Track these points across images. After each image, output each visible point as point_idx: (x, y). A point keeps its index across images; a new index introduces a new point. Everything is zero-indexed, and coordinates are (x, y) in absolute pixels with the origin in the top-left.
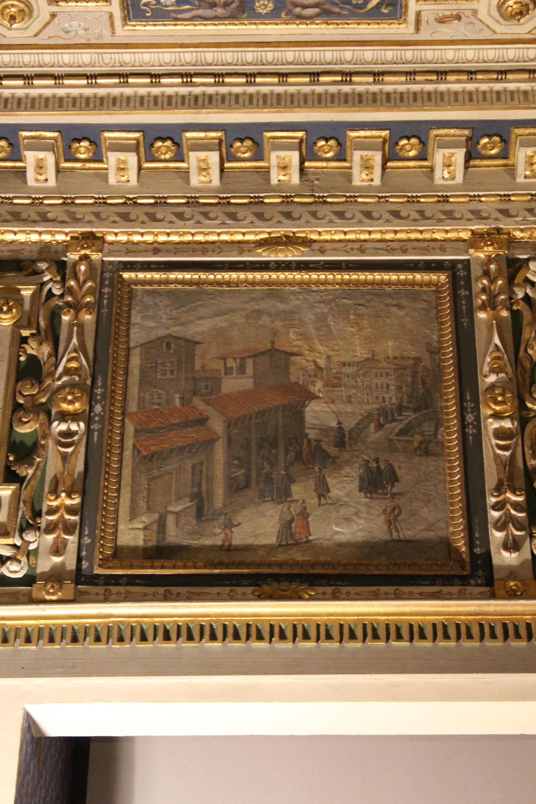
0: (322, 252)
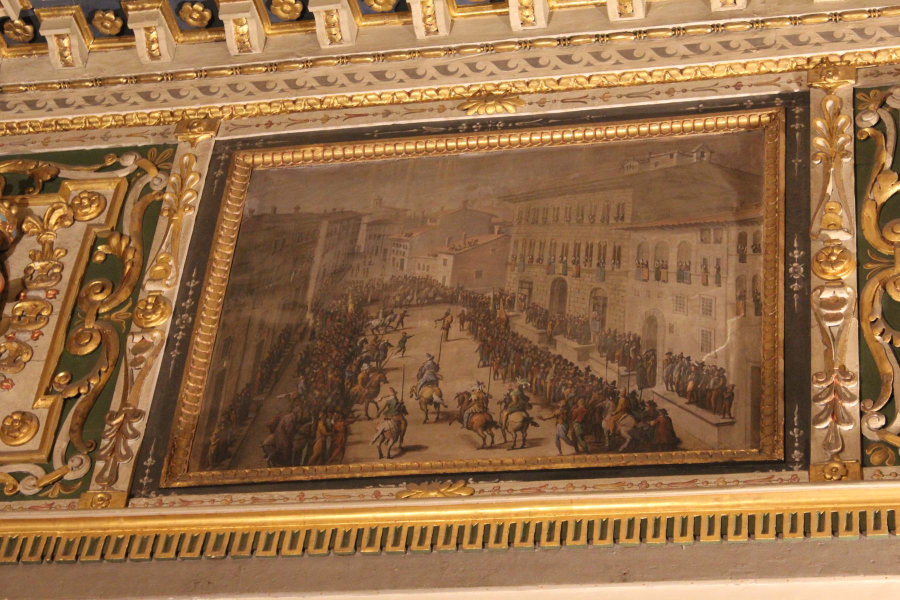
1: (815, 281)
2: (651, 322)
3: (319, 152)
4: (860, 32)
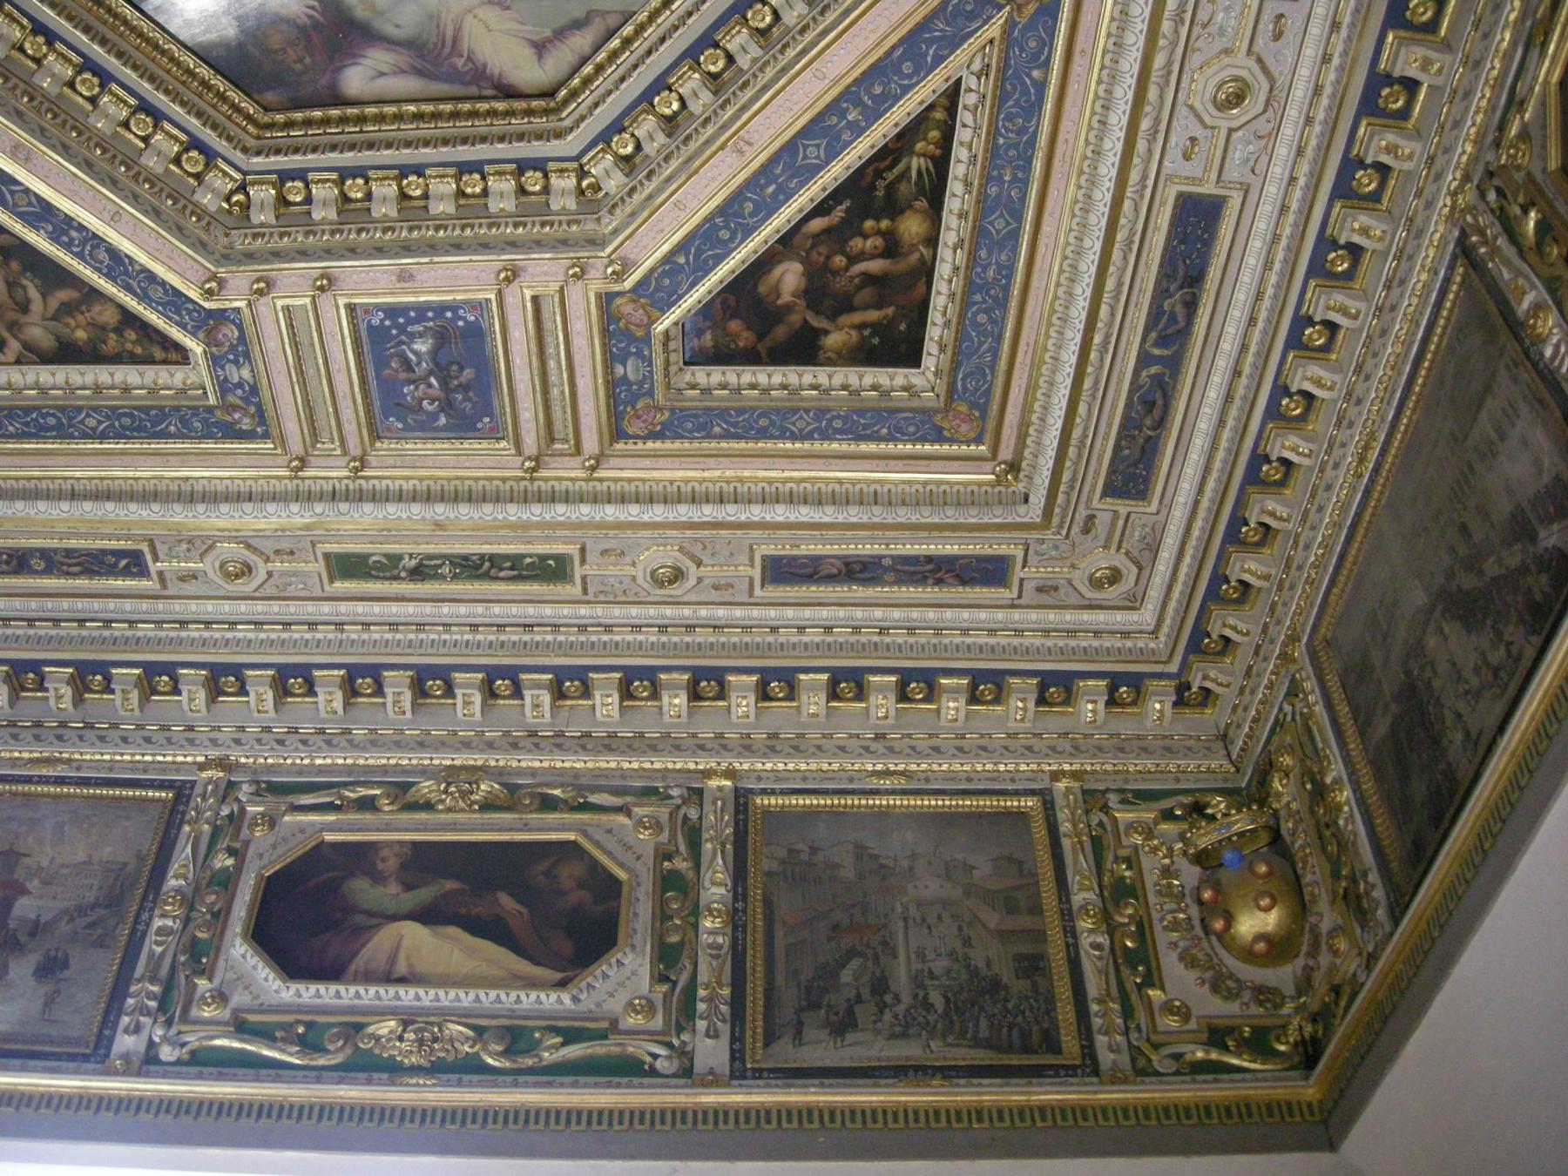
0: (78, 769)
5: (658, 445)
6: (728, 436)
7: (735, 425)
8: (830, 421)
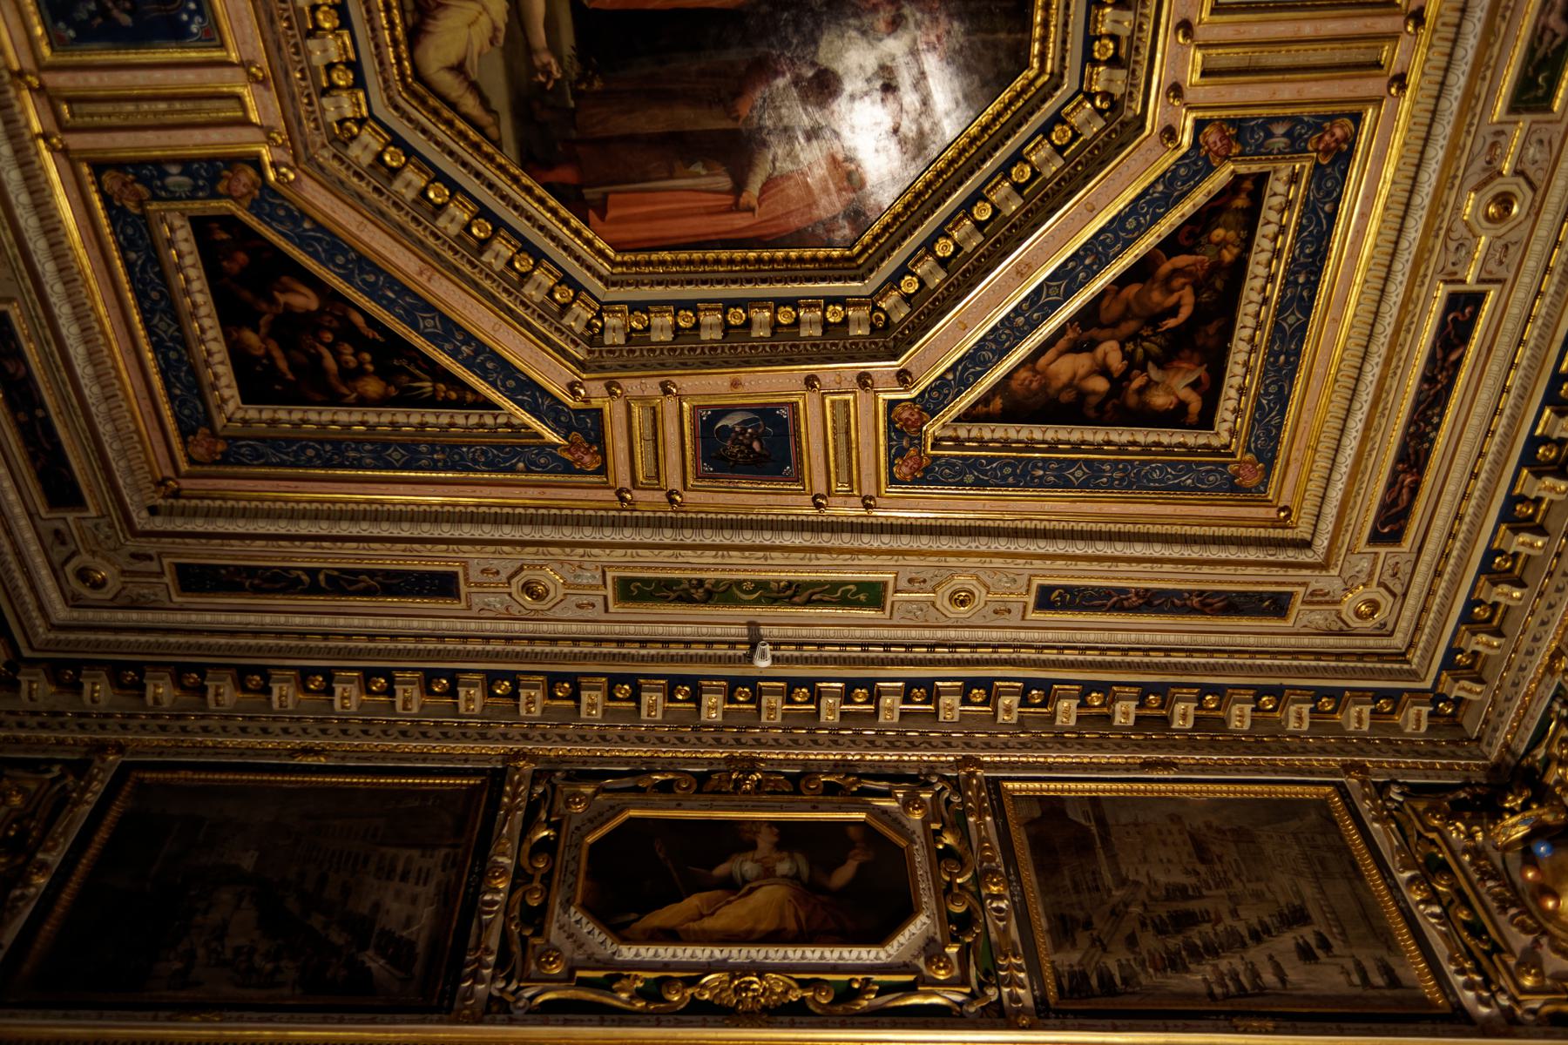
1: (483, 888)
2: (377, 906)
3: (190, 775)
4: (543, 736)
5: (98, 205)
6: (129, 266)
7: (143, 270)
8: (175, 349)
